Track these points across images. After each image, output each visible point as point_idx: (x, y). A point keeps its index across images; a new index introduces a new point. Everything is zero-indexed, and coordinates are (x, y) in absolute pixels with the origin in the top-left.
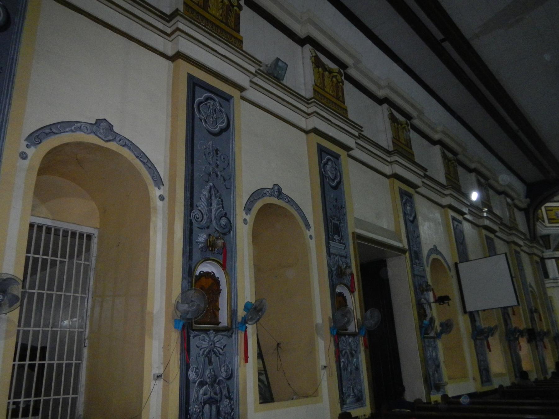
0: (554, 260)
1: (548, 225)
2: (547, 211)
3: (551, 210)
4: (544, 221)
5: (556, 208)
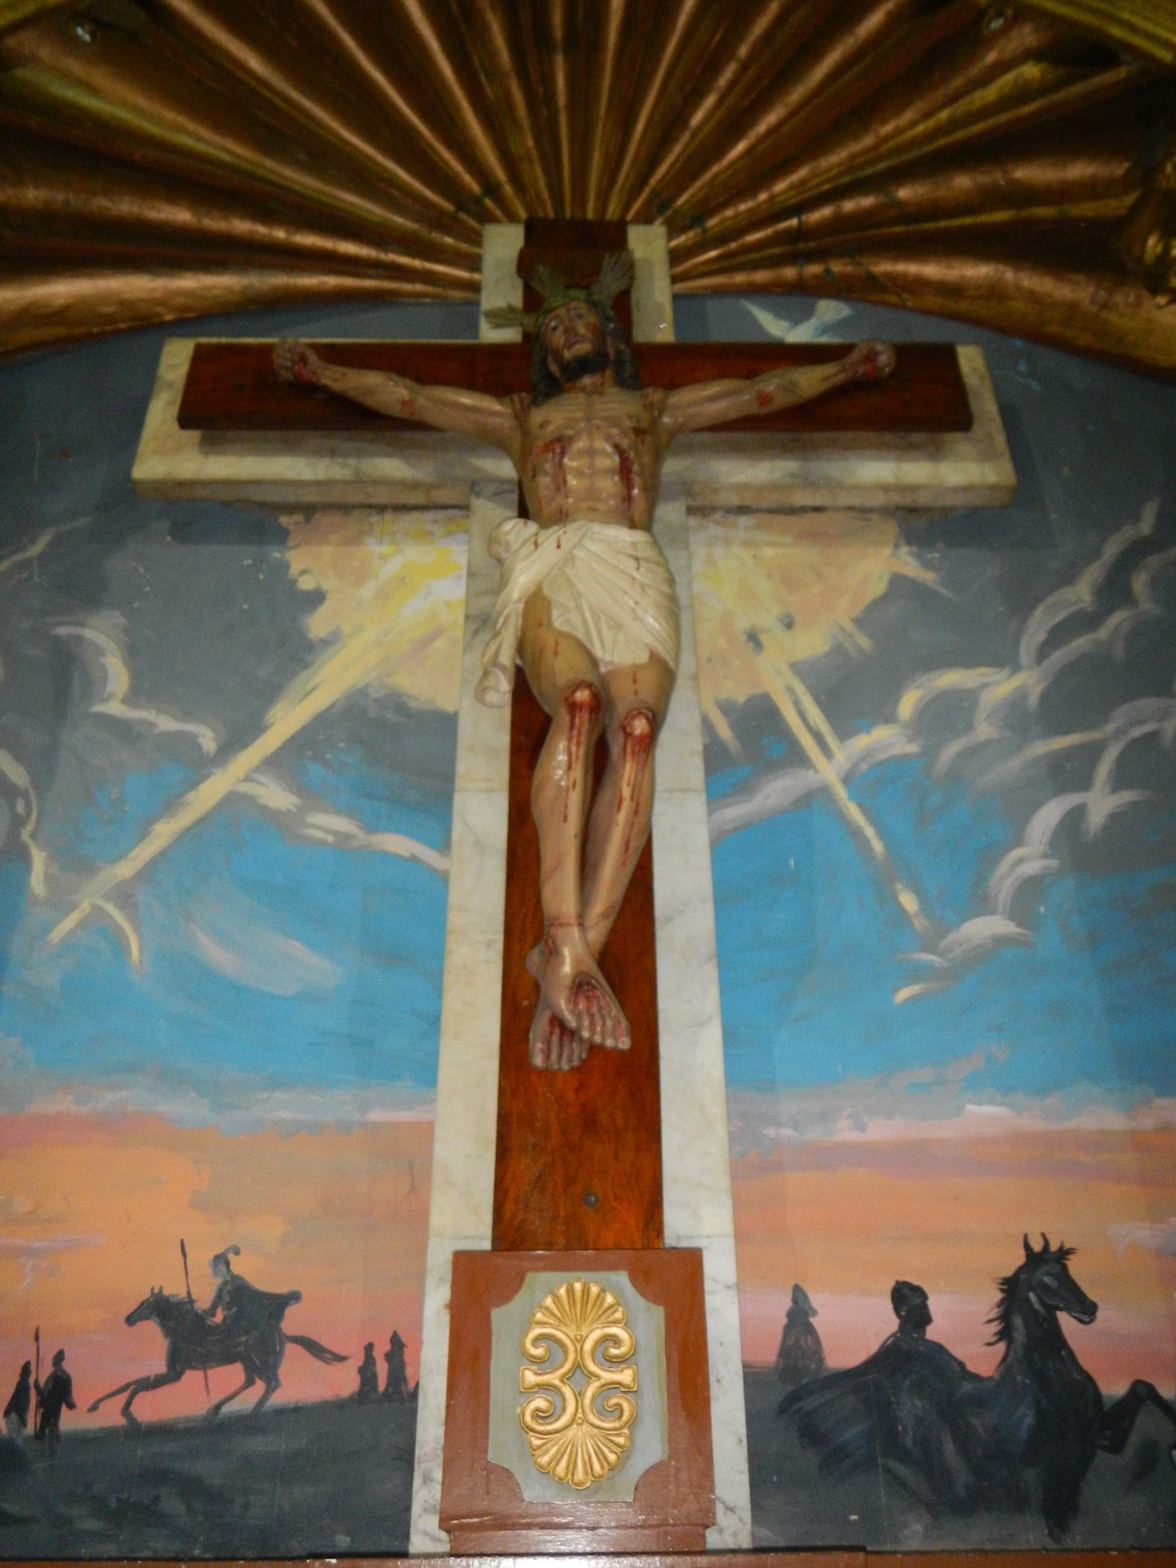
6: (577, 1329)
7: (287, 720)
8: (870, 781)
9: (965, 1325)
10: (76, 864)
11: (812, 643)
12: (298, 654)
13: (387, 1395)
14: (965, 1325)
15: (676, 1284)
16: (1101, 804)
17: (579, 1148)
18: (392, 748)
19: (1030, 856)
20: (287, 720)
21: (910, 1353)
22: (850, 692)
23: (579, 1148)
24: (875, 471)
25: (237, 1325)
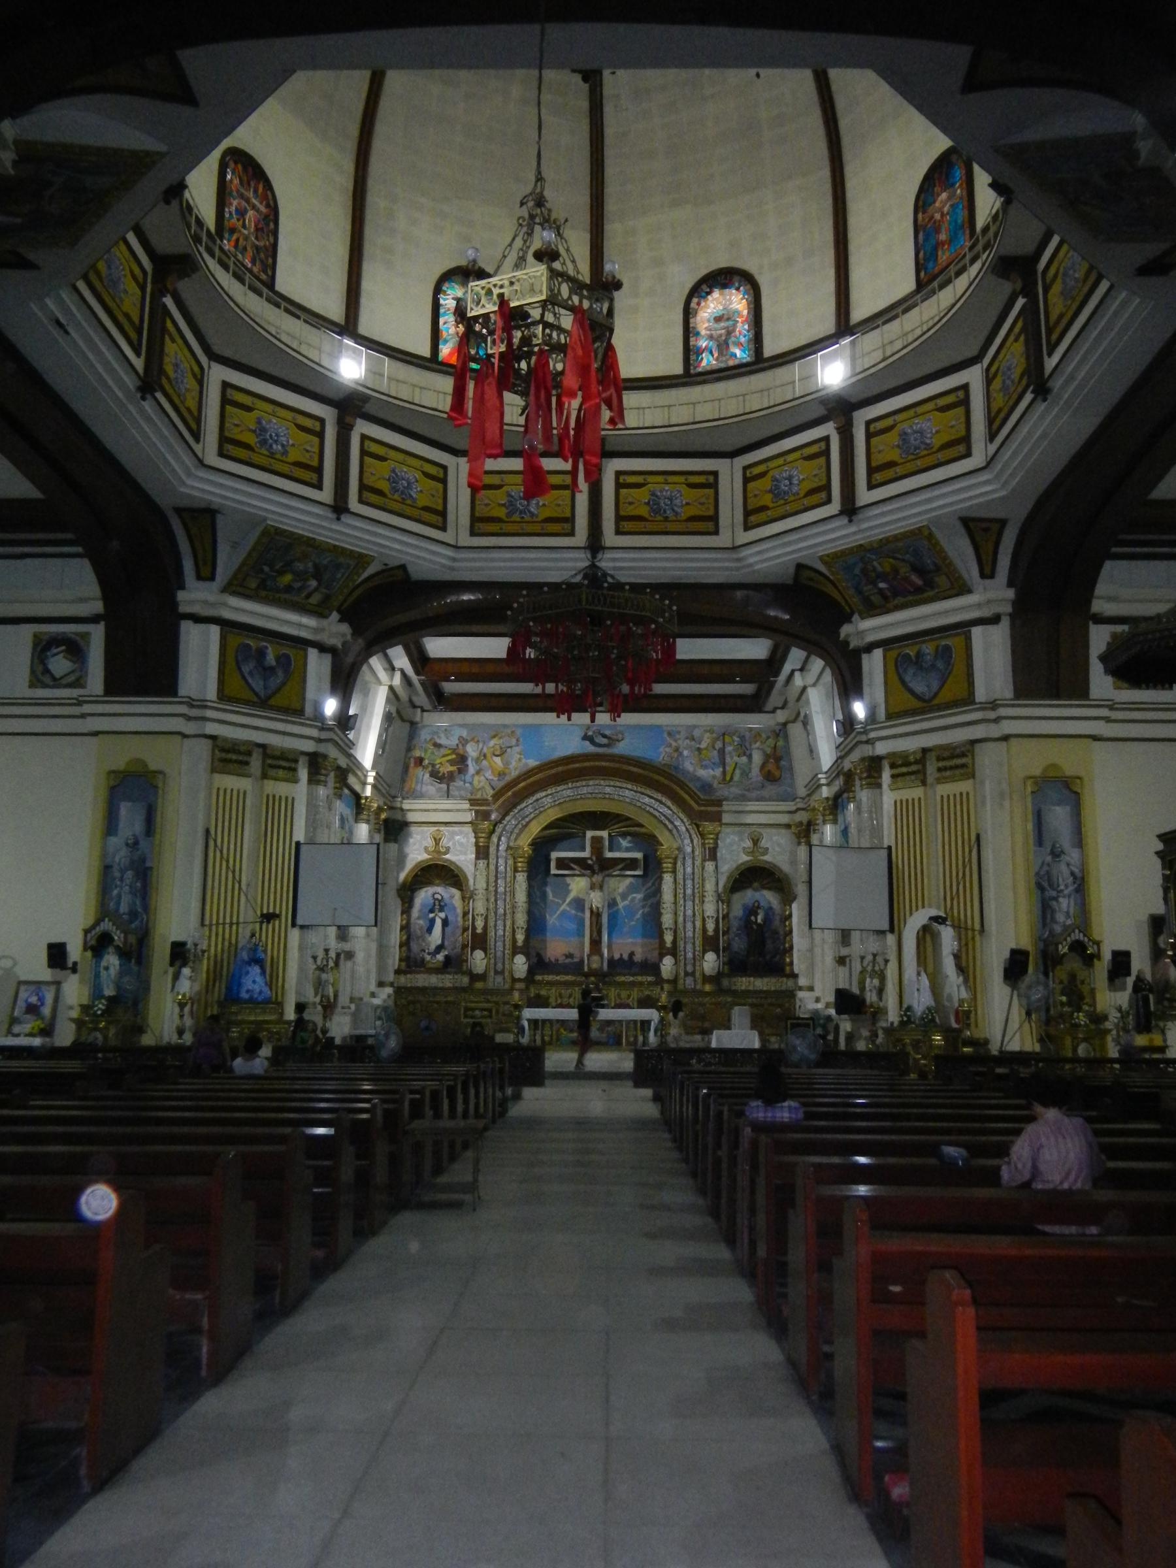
0: (215, 631)
1: (212, 459)
2: (225, 401)
3: (249, 409)
4: (197, 437)
5: (269, 408)
6: (596, 958)
7: (568, 900)
8: (624, 907)
9: (625, 957)
10: (551, 916)
11: (620, 890)
12: (568, 892)
13: (582, 961)
14: (625, 957)
15: (602, 956)
16: (647, 910)
17: (596, 943)
18: (579, 904)
19: (638, 916)
20: (568, 900)
21: (621, 959)
22: (624, 896)
23: (596, 943)
24: (628, 873)
25: (570, 956)
